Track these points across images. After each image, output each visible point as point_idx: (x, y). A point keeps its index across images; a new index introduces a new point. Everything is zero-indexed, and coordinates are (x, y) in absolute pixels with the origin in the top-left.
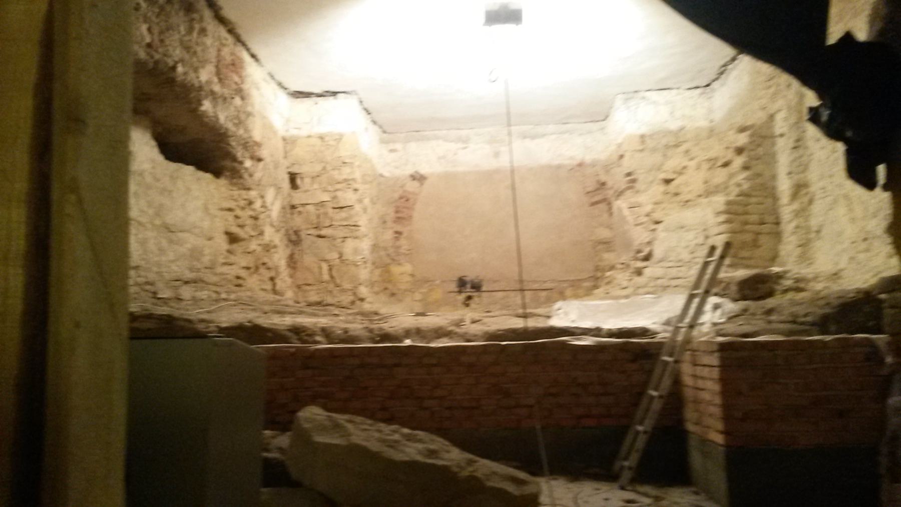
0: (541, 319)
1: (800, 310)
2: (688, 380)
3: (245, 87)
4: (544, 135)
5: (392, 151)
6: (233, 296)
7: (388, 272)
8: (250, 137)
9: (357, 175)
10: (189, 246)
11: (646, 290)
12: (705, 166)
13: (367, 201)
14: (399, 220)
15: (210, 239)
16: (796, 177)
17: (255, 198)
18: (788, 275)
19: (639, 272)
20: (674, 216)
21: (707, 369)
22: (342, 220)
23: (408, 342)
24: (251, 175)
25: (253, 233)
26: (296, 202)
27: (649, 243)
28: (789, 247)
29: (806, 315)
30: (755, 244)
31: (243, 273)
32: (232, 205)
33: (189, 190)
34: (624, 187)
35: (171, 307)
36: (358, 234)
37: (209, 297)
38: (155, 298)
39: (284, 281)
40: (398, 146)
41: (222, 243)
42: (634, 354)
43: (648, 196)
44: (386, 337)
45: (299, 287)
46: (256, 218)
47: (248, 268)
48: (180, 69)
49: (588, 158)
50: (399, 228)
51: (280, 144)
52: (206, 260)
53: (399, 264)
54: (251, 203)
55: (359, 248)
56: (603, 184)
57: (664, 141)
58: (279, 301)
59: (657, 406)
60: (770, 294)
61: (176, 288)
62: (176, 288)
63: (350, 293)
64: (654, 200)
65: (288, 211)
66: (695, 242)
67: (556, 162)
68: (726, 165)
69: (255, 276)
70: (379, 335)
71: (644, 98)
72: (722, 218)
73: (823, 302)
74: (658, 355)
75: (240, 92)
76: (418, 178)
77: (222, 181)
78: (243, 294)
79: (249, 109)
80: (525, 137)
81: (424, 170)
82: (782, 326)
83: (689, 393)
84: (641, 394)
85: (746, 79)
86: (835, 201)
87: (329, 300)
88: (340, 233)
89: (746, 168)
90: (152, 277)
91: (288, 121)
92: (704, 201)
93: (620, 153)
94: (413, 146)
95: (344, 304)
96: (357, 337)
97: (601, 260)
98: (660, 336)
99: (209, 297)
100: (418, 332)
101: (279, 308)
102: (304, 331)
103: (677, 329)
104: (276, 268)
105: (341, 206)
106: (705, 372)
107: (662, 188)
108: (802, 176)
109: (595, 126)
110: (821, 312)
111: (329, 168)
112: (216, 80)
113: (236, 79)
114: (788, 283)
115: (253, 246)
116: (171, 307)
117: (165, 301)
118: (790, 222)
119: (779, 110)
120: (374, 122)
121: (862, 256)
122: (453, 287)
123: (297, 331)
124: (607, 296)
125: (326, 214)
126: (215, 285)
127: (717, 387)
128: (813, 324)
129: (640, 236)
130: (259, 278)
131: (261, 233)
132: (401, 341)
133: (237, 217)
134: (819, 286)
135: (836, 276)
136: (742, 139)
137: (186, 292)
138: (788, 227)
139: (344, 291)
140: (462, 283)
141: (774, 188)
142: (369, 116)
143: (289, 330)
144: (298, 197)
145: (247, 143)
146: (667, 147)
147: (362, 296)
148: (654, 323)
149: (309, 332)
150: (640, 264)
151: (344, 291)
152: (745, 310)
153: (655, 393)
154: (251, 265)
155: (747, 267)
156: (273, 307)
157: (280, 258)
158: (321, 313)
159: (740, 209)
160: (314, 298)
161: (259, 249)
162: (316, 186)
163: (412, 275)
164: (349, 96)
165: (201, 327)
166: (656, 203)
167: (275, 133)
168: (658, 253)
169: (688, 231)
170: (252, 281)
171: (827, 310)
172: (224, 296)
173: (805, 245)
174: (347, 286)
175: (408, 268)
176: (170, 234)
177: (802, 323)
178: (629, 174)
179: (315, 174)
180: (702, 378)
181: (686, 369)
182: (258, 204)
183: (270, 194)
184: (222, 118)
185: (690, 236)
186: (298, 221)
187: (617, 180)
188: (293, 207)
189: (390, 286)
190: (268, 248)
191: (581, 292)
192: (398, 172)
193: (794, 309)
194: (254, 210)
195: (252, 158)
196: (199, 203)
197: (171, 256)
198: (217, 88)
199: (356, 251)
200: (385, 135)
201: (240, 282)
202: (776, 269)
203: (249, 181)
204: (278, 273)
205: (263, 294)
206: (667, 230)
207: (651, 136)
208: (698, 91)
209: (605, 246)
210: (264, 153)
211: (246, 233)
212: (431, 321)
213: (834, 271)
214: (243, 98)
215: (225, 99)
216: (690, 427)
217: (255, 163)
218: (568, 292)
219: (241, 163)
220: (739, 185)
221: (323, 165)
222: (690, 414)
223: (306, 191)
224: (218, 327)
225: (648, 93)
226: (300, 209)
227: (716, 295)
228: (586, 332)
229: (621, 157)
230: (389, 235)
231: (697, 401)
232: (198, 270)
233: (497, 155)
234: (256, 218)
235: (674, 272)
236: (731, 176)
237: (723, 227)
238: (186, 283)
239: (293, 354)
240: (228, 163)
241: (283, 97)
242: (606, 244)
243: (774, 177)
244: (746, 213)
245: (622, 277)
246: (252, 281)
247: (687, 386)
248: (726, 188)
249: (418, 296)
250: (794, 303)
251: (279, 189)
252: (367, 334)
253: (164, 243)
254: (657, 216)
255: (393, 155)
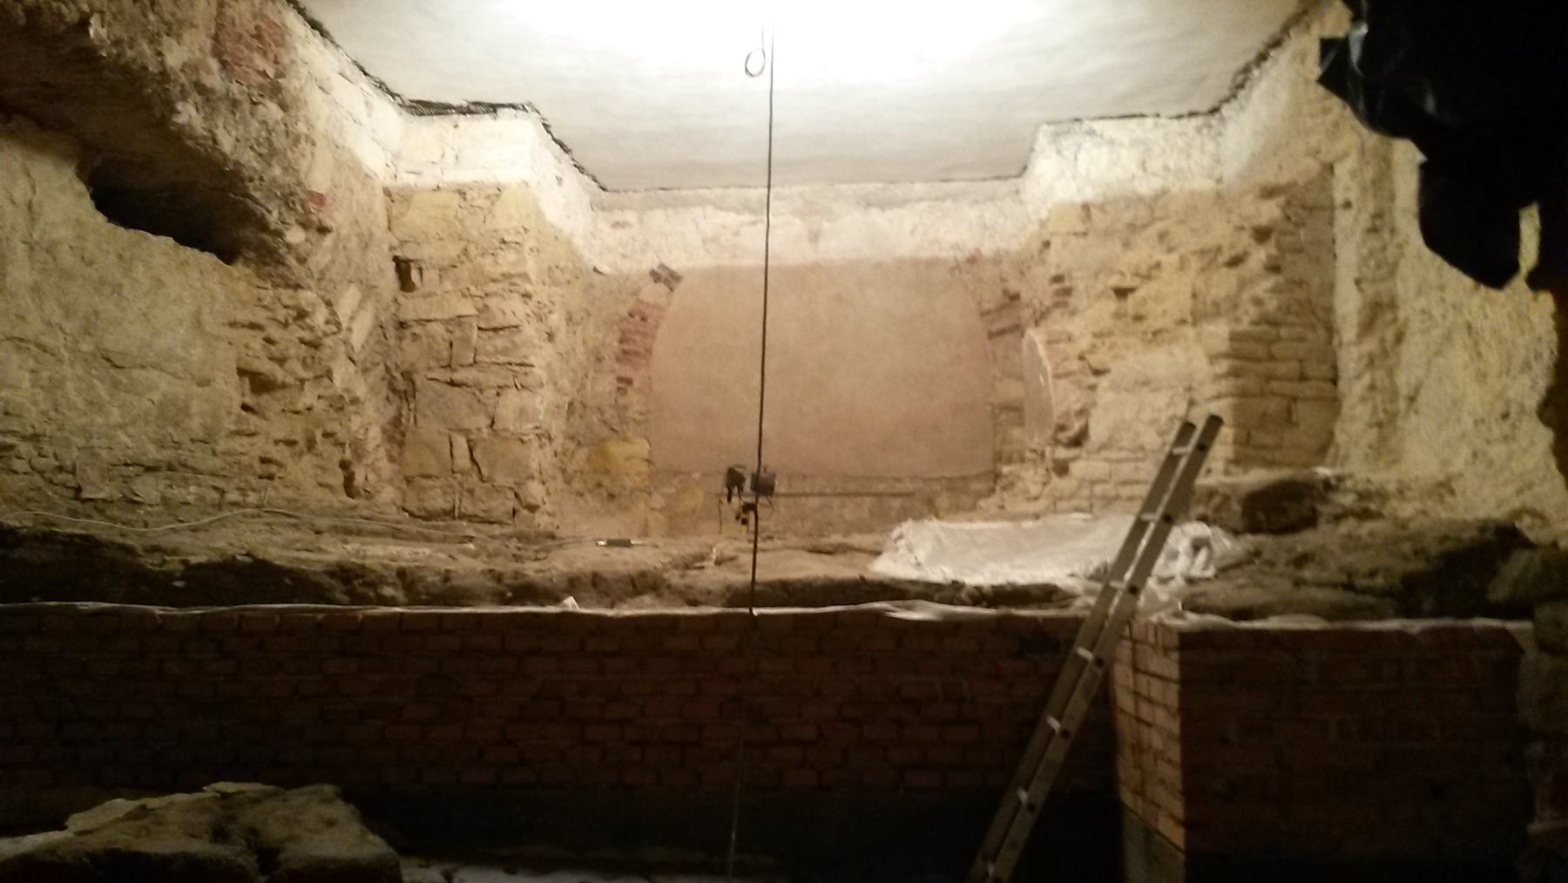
0: (860, 558)
1: (1360, 561)
2: (1125, 700)
3: (291, 84)
4: (904, 202)
5: (617, 225)
6: (252, 498)
7: (604, 454)
8: (299, 184)
9: (531, 267)
10: (156, 396)
11: (1075, 503)
12: (1195, 264)
13: (556, 319)
14: (625, 356)
15: (204, 383)
16: (1370, 290)
17: (313, 305)
18: (1349, 483)
19: (1062, 469)
20: (1132, 360)
21: (1156, 684)
22: (497, 352)
23: (570, 603)
24: (302, 261)
25: (303, 374)
26: (408, 315)
27: (1083, 412)
28: (1354, 425)
29: (1373, 574)
30: (1288, 418)
31: (277, 453)
32: (261, 316)
33: (159, 283)
34: (1048, 302)
35: (113, 519)
36: (529, 380)
37: (201, 498)
38: (77, 498)
39: (376, 469)
40: (630, 216)
41: (232, 391)
42: (1020, 640)
43: (1088, 318)
44: (527, 592)
45: (409, 481)
46: (315, 345)
47: (291, 443)
48: (95, 29)
49: (987, 249)
50: (627, 372)
51: (379, 203)
52: (195, 424)
53: (626, 440)
54: (302, 315)
55: (535, 407)
56: (1015, 297)
57: (1128, 216)
58: (354, 508)
59: (1057, 753)
60: (1310, 521)
61: (126, 479)
62: (126, 479)
63: (511, 495)
64: (1096, 330)
65: (391, 332)
66: (1171, 412)
67: (925, 254)
68: (1235, 262)
69: (307, 458)
70: (513, 588)
71: (1091, 133)
72: (1223, 366)
73: (1406, 547)
74: (1070, 643)
75: (275, 90)
76: (665, 277)
77: (238, 269)
78: (274, 494)
79: (302, 128)
80: (869, 205)
81: (677, 263)
82: (1321, 595)
83: (1125, 726)
84: (1034, 722)
85: (1284, 96)
86: (1448, 338)
87: (468, 506)
88: (493, 379)
89: (1274, 268)
90: (71, 456)
91: (397, 156)
92: (1190, 331)
93: (1046, 237)
94: (657, 218)
95: (495, 515)
96: (466, 590)
97: (1004, 440)
98: (1078, 603)
99: (201, 498)
100: (596, 585)
101: (351, 523)
102: (357, 576)
103: (1108, 592)
104: (358, 448)
105: (495, 324)
106: (1155, 689)
107: (1112, 305)
108: (1382, 287)
109: (1003, 187)
110: (1401, 567)
111: (472, 250)
112: (214, 64)
113: (260, 63)
114: (1348, 500)
115: (308, 398)
116: (113, 519)
117: (101, 506)
118: (1358, 377)
119: (1345, 155)
120: (581, 169)
121: (1497, 451)
122: (719, 485)
123: (345, 574)
124: (1002, 513)
125: (466, 341)
126: (213, 474)
127: (1175, 727)
128: (1387, 593)
129: (1064, 398)
130: (315, 461)
131: (329, 374)
132: (557, 600)
133: (269, 341)
134: (1407, 510)
135: (1444, 487)
136: (1269, 211)
137: (149, 489)
138: (1353, 389)
139: (498, 490)
140: (734, 479)
141: (1329, 310)
142: (567, 156)
143: (331, 574)
144: (412, 307)
145: (292, 194)
146: (1132, 227)
147: (532, 501)
148: (1072, 575)
149: (373, 577)
150: (1062, 453)
151: (498, 490)
152: (1257, 553)
153: (1055, 724)
154: (299, 437)
155: (1269, 464)
156: (338, 522)
157: (369, 423)
158: (440, 534)
159: (1260, 350)
160: (439, 502)
161: (319, 406)
162: (448, 286)
163: (649, 462)
164: (521, 113)
165: (150, 562)
166: (1095, 335)
167: (366, 178)
168: (1097, 432)
169: (1157, 390)
170: (302, 470)
171: (1416, 565)
172: (233, 496)
173: (1385, 425)
174: (502, 479)
175: (641, 447)
176: (113, 372)
177: (1364, 591)
178: (1058, 279)
179: (446, 263)
180: (1150, 701)
181: (1122, 674)
182: (320, 317)
183: (348, 300)
184: (226, 144)
185: (1161, 400)
186: (411, 353)
187: (1037, 290)
188: (402, 325)
189: (606, 482)
190: (339, 404)
191: (966, 500)
192: (626, 266)
193: (1348, 559)
194: (311, 329)
195: (305, 226)
196: (185, 311)
197: (116, 416)
198: (214, 79)
199: (522, 413)
200: (604, 195)
201: (273, 469)
202: (1323, 471)
203: (298, 271)
204: (359, 453)
205: (321, 493)
206: (1115, 387)
207: (1102, 208)
208: (1195, 122)
209: (1012, 414)
210: (337, 218)
211: (292, 373)
212: (645, 556)
213: (1441, 477)
214: (284, 107)
215: (235, 104)
216: (1127, 797)
217: (314, 236)
218: (943, 501)
219: (279, 234)
220: (1258, 302)
221: (463, 244)
222: (1127, 770)
223: (431, 294)
224: (185, 562)
225: (1098, 126)
226: (417, 330)
227: (1203, 519)
228: (930, 591)
229: (1047, 244)
230: (607, 384)
231: (1139, 748)
232: (178, 445)
233: (815, 237)
234: (315, 345)
235: (1126, 470)
236: (1243, 284)
237: (1225, 385)
238: (149, 469)
239: (320, 625)
240: (248, 233)
241: (387, 114)
242: (1014, 410)
243: (1330, 288)
244: (1272, 358)
245: (1030, 477)
246: (302, 470)
247: (1122, 711)
248: (1235, 306)
249: (658, 501)
250: (1352, 544)
251: (369, 289)
252: (491, 584)
253: (102, 390)
254: (1095, 360)
255: (619, 233)
